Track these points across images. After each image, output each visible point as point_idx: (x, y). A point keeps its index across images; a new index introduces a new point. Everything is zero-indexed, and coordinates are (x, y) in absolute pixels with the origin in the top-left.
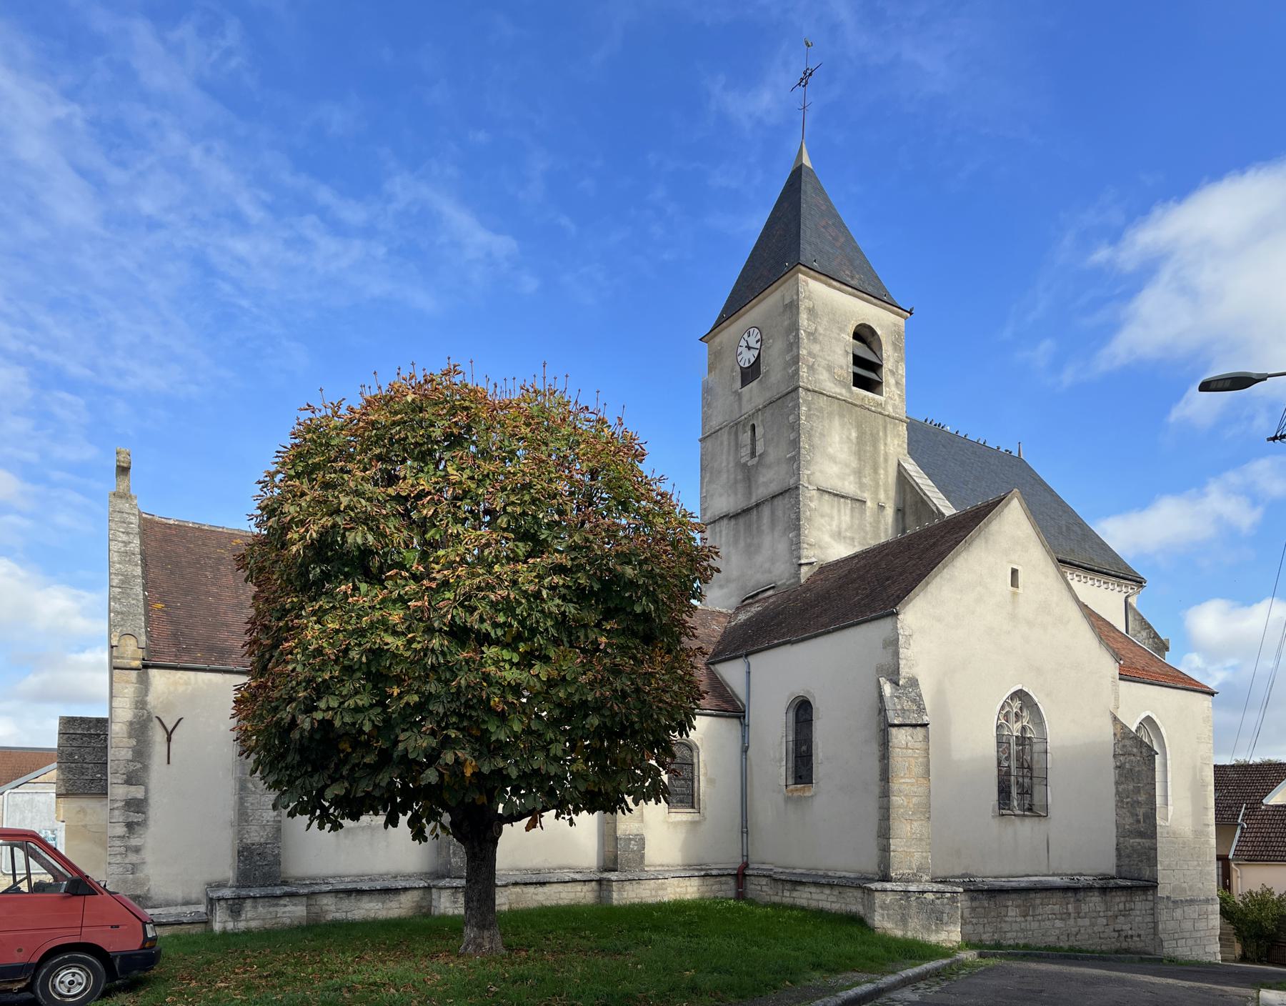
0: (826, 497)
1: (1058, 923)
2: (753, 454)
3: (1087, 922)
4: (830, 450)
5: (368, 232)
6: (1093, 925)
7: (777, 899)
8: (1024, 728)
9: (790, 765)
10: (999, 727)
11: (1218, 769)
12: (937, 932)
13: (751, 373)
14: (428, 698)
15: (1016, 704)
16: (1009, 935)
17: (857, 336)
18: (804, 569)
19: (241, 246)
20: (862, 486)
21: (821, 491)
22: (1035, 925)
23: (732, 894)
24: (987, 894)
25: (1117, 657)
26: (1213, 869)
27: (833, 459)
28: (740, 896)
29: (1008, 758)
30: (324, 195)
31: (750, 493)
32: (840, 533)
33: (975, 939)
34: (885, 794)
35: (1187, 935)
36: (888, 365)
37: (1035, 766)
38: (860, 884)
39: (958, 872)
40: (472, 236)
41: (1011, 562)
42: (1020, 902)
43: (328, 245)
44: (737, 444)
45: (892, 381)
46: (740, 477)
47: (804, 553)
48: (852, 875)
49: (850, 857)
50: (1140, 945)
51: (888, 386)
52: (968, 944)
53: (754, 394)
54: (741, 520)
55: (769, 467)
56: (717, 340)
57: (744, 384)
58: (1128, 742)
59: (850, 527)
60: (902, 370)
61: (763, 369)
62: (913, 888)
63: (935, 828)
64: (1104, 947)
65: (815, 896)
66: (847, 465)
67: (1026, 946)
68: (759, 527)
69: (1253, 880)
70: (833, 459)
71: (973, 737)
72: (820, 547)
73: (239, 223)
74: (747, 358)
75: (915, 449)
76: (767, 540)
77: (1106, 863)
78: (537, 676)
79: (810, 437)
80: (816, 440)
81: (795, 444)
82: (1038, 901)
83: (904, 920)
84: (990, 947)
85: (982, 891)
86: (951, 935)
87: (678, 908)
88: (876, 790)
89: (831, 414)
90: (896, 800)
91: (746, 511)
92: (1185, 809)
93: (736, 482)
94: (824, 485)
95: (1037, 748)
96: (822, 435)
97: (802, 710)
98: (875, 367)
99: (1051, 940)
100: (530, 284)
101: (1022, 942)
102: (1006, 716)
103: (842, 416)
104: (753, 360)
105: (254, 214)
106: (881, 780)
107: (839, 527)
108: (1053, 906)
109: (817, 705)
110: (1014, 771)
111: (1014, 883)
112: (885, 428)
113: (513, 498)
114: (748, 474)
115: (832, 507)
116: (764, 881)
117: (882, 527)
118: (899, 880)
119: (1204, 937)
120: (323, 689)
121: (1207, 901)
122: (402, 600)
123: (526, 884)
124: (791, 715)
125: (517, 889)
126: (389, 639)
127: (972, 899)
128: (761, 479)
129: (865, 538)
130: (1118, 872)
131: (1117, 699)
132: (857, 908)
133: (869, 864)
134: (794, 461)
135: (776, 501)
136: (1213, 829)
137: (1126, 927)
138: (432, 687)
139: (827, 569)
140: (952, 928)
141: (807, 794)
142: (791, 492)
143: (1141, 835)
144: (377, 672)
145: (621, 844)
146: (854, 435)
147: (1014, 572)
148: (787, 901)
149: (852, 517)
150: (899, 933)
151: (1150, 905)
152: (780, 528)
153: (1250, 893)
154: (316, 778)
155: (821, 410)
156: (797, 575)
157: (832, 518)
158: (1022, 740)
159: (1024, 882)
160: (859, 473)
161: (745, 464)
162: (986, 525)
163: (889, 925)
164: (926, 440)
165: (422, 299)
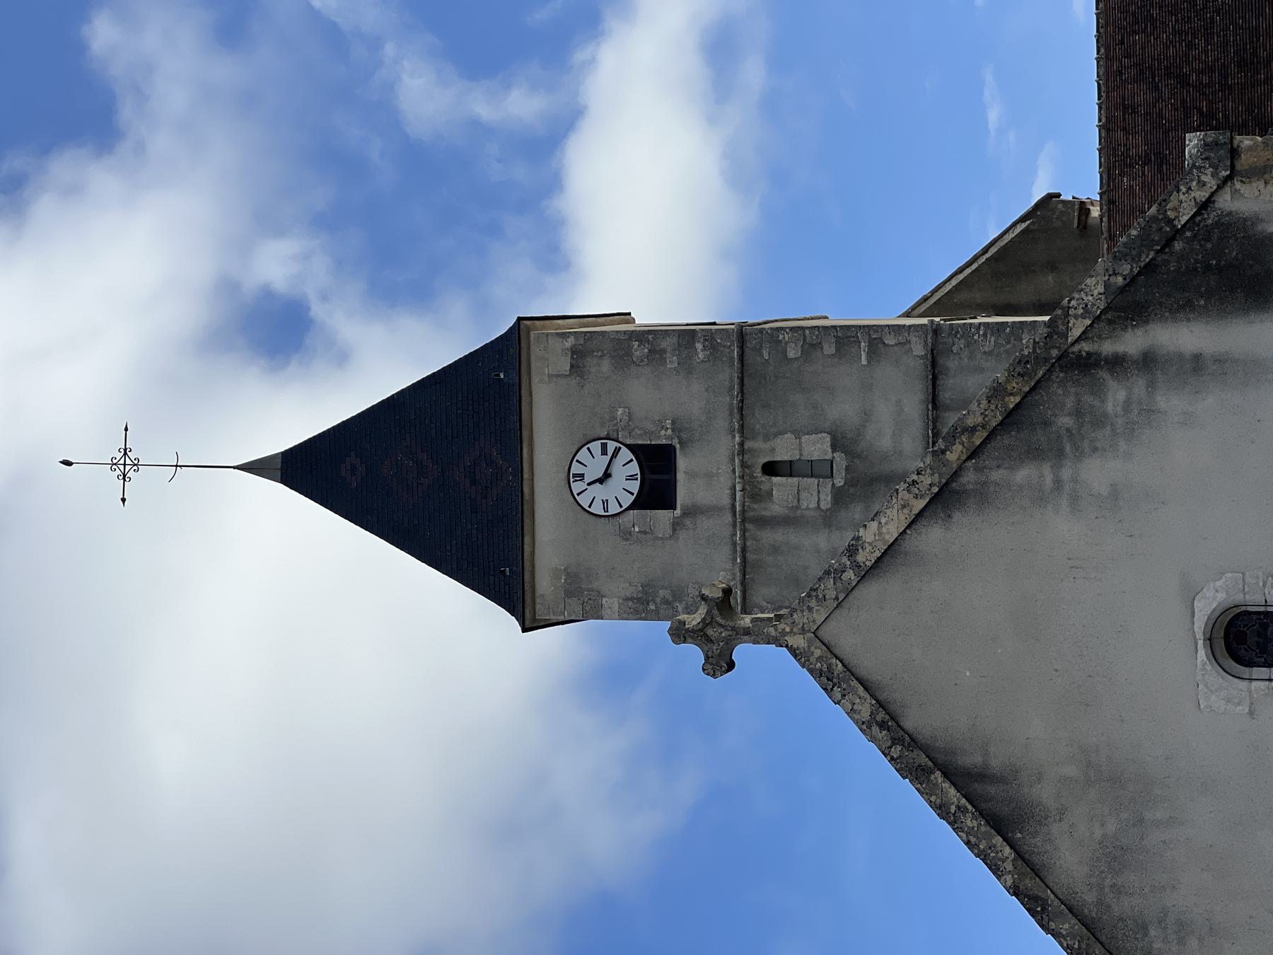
13: (657, 487)
53: (703, 476)
55: (867, 415)
74: (627, 473)
104: (635, 468)
128: (886, 443)
135: (945, 396)
161: (840, 497)
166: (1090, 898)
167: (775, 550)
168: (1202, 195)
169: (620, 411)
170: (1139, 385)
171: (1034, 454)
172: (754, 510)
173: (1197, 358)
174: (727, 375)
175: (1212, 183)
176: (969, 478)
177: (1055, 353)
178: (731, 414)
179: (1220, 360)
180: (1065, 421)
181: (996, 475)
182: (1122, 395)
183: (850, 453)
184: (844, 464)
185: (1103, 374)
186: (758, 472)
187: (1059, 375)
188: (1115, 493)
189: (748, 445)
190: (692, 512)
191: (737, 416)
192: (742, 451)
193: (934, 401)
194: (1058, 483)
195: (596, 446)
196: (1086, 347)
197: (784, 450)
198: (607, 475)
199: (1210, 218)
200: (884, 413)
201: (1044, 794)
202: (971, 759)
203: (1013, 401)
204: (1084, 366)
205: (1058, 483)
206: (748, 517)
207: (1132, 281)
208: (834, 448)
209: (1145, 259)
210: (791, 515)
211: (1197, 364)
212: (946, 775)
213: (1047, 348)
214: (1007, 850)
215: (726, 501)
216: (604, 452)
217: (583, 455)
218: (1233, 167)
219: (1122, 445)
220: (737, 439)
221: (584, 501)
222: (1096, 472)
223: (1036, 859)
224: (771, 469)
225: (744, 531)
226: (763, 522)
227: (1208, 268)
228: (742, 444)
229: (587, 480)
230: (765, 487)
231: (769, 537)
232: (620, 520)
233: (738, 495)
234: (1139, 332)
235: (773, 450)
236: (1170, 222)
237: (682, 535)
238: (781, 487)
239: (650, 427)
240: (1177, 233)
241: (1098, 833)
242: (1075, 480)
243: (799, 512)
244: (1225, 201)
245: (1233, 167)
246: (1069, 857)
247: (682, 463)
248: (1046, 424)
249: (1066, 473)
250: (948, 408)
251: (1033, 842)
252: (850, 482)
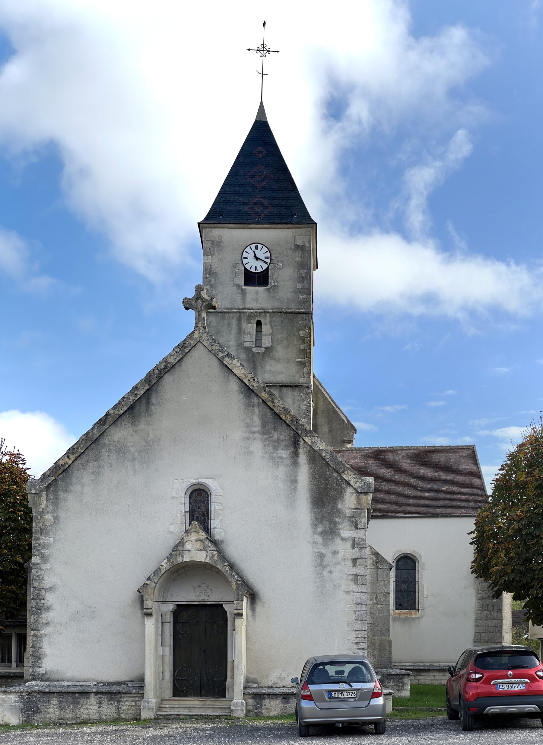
55: (278, 361)
57: (247, 283)
104: (260, 270)
128: (268, 367)
135: (284, 390)
161: (248, 349)
166: (107, 441)
167: (229, 325)
168: (352, 483)
169: (281, 265)
170: (288, 462)
171: (264, 424)
172: (244, 317)
173: (296, 481)
175: (356, 486)
176: (256, 400)
177: (300, 432)
178: (279, 309)
179: (295, 488)
180: (276, 436)
181: (256, 410)
182: (284, 456)
183: (264, 354)
184: (260, 352)
185: (292, 449)
186: (257, 319)
187: (292, 433)
188: (250, 453)
189: (268, 315)
190: (243, 292)
191: (278, 311)
192: (265, 313)
193: (282, 386)
194: (254, 432)
195: (268, 255)
196: (302, 443)
197: (266, 328)
198: (257, 259)
199: (344, 485)
200: (279, 367)
201: (142, 426)
202: (154, 399)
203: (283, 417)
204: (295, 443)
205: (254, 432)
206: (241, 314)
207: (324, 459)
208: (266, 348)
209: (331, 463)
210: (242, 331)
211: (294, 481)
212: (148, 390)
213: (302, 429)
214: (122, 412)
215: (247, 306)
216: (266, 258)
217: (265, 249)
218: (361, 493)
219: (267, 456)
220: (270, 311)
221: (248, 249)
222: (257, 446)
223: (119, 422)
224: (259, 323)
225: (236, 313)
226: (239, 320)
227: (327, 485)
228: (268, 312)
229: (256, 251)
230: (252, 321)
231: (234, 322)
232: (241, 264)
233: (250, 311)
234: (305, 461)
235: (266, 324)
236: (343, 472)
237: (235, 288)
238: (252, 327)
239: (275, 276)
240: (339, 474)
241: (129, 444)
242: (254, 439)
243: (243, 334)
244: (349, 490)
245: (361, 493)
246: (120, 434)
247: (261, 289)
248: (275, 429)
249: (257, 435)
250: (280, 391)
251: (125, 421)
252: (254, 354)
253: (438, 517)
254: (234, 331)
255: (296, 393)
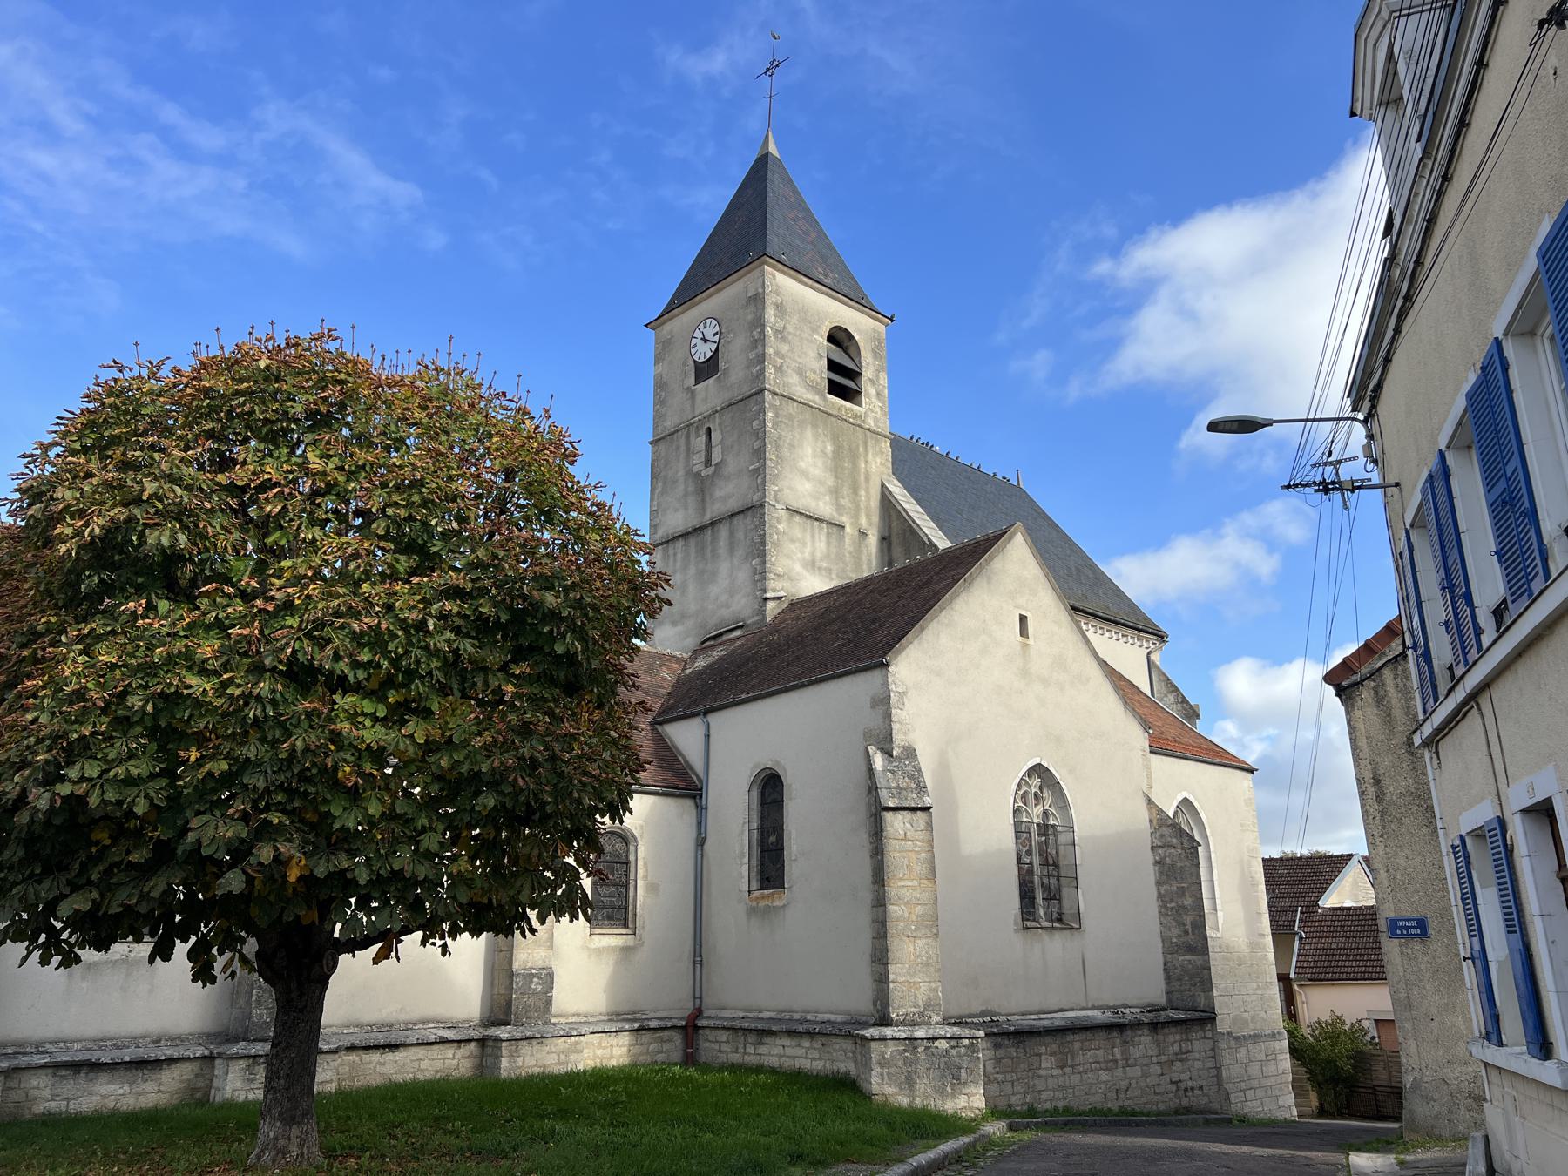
0: (797, 518)
1: (1104, 1076)
2: (708, 462)
3: (1136, 1072)
4: (802, 464)
5: (225, 161)
6: (1145, 1075)
7: (736, 1058)
8: (1045, 813)
9: (754, 862)
10: (1016, 811)
11: (1268, 863)
12: (954, 1096)
13: (707, 369)
14: (243, 766)
15: (1035, 782)
16: (1044, 1096)
17: (831, 338)
18: (770, 605)
19: (45, 160)
20: (839, 508)
21: (792, 511)
22: (1076, 1079)
23: (677, 1056)
24: (1014, 1038)
25: (1146, 725)
26: (1275, 991)
27: (805, 475)
28: (689, 1059)
29: (1029, 853)
30: (170, 113)
31: (704, 509)
32: (813, 563)
33: (1002, 1104)
34: (880, 902)
35: (1255, 1083)
36: (867, 374)
37: (1062, 863)
38: (849, 1031)
39: (976, 1009)
40: (365, 180)
41: (1017, 607)
42: (1055, 1047)
43: (167, 169)
44: (688, 449)
45: (873, 391)
46: (691, 488)
47: (771, 584)
48: (839, 1018)
49: (839, 995)
50: (1204, 1100)
51: (868, 395)
52: (995, 1112)
53: (710, 394)
54: (692, 541)
56: (667, 327)
57: (698, 380)
58: (1166, 831)
59: (827, 557)
60: (883, 380)
61: (722, 366)
62: (920, 1033)
63: (945, 951)
64: (1161, 1107)
65: (789, 1051)
66: (821, 483)
67: (1067, 1110)
68: (713, 551)
69: (1326, 1004)
70: (805, 475)
71: (985, 826)
72: (790, 579)
73: (48, 133)
74: (703, 351)
75: (896, 472)
76: (724, 567)
77: (1153, 989)
78: (411, 736)
79: (778, 447)
80: (785, 452)
81: (760, 453)
82: (1077, 1046)
83: (910, 1082)
84: (1021, 1115)
85: (1007, 1034)
86: (971, 1100)
87: (599, 1079)
88: (867, 896)
89: (802, 423)
90: (894, 910)
91: (698, 530)
92: (1237, 917)
93: (686, 495)
94: (794, 505)
95: (1063, 838)
96: (792, 446)
97: (770, 787)
98: (854, 375)
99: (1096, 1100)
100: (435, 240)
101: (1061, 1105)
102: (1024, 796)
103: (815, 426)
104: (709, 354)
105: (71, 125)
106: (875, 883)
107: (813, 554)
108: (1094, 1051)
109: (788, 780)
110: (1037, 870)
111: (1046, 1021)
112: (866, 443)
113: (396, 498)
114: (702, 486)
115: (805, 530)
116: (723, 1035)
117: (864, 558)
118: (902, 1023)
119: (1272, 1086)
120: (79, 750)
121: (1274, 1036)
122: (221, 626)
123: (367, 1048)
124: (755, 793)
125: (353, 1057)
126: (192, 680)
127: (997, 1047)
128: (718, 494)
129: (844, 571)
130: (1169, 1000)
131: (1149, 776)
132: (846, 1066)
133: (861, 1001)
134: (759, 473)
135: (735, 520)
136: (1269, 939)
137: (1185, 1076)
138: (251, 751)
139: (798, 606)
140: (972, 1089)
141: (777, 903)
142: (754, 510)
143: (1191, 949)
144: (168, 727)
145: (518, 983)
146: (829, 448)
147: (1023, 619)
148: (751, 1060)
149: (828, 543)
150: (904, 1101)
151: (1208, 1044)
152: (740, 552)
153: (1319, 1023)
154: (46, 884)
155: (790, 417)
156: (762, 611)
157: (804, 544)
158: (1044, 829)
159: (1058, 1019)
160: (835, 492)
161: (698, 474)
162: (988, 562)
163: (890, 1090)
164: (912, 460)
165: (291, 244)
167: (678, 448)
174: (746, 391)
253: (803, 686)
254: (682, 456)
255: (748, 520)
